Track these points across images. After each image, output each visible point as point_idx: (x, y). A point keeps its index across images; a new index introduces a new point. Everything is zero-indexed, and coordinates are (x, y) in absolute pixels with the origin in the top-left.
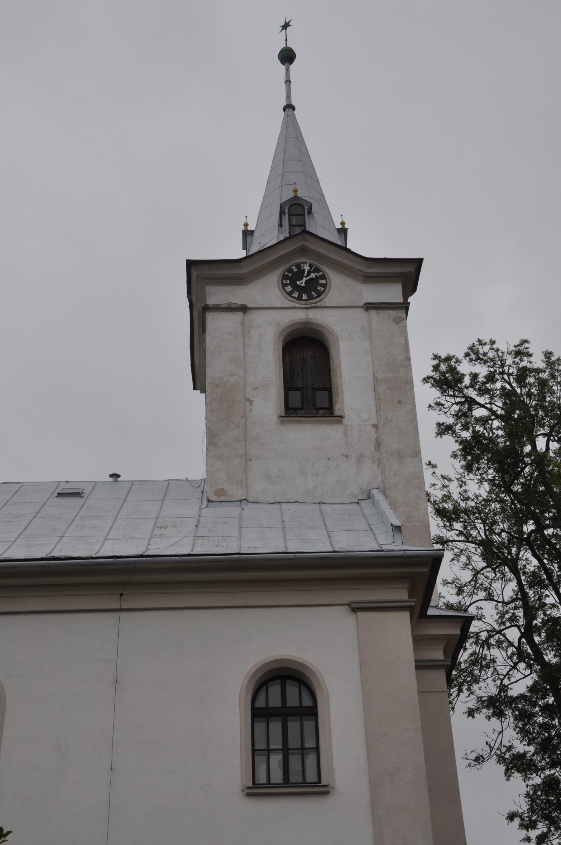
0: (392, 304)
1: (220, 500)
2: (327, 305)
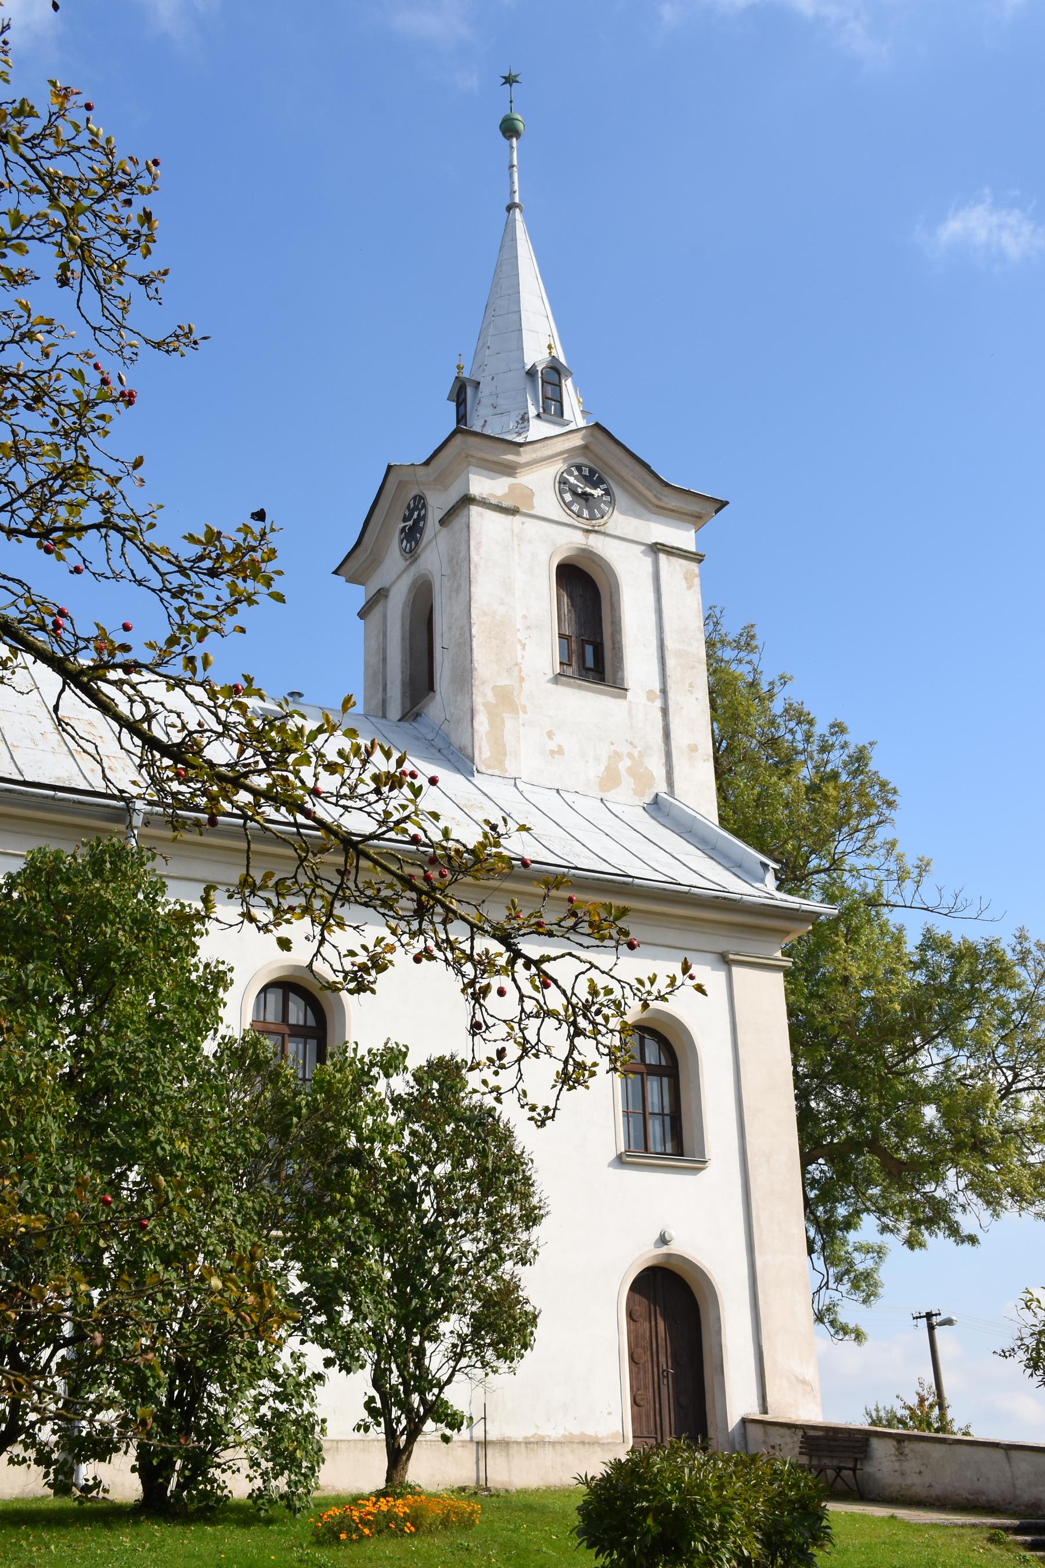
0: (686, 551)
1: (490, 772)
2: (611, 532)
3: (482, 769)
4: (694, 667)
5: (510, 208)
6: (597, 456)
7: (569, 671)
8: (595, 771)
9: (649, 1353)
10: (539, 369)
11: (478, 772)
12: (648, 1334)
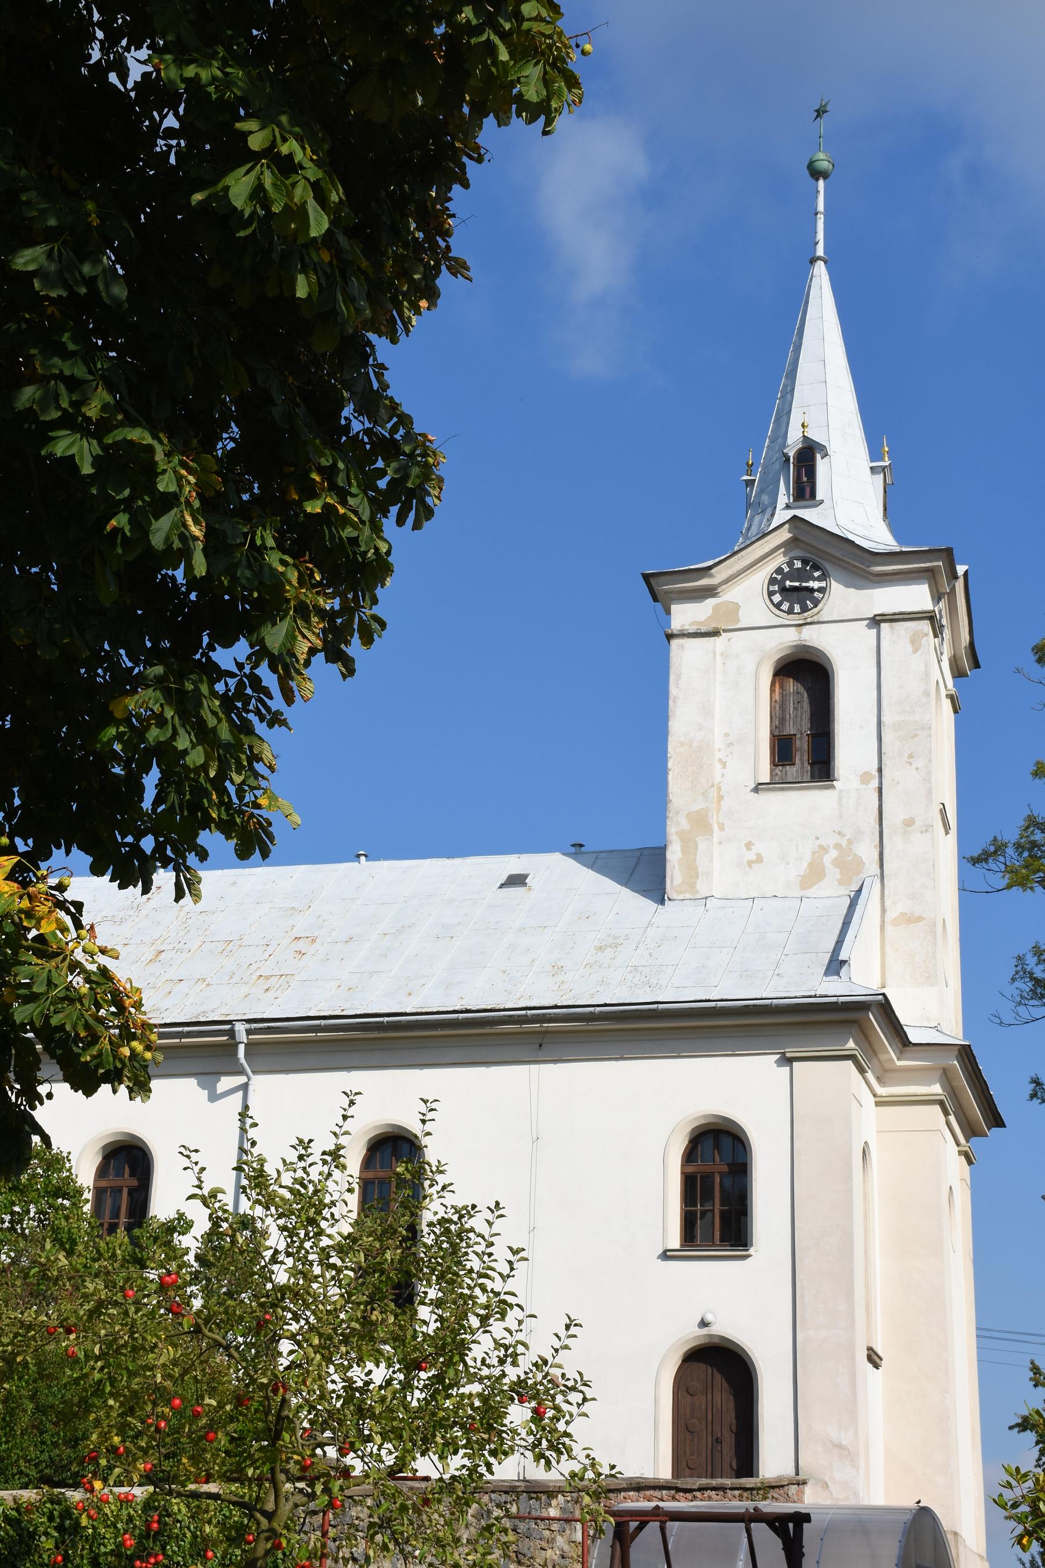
1: (681, 897)
2: (826, 619)
3: (673, 896)
4: (916, 736)
5: (813, 260)
6: (808, 544)
7: (792, 771)
8: (798, 869)
9: (704, 1423)
10: (791, 454)
11: (670, 899)
12: (704, 1406)
